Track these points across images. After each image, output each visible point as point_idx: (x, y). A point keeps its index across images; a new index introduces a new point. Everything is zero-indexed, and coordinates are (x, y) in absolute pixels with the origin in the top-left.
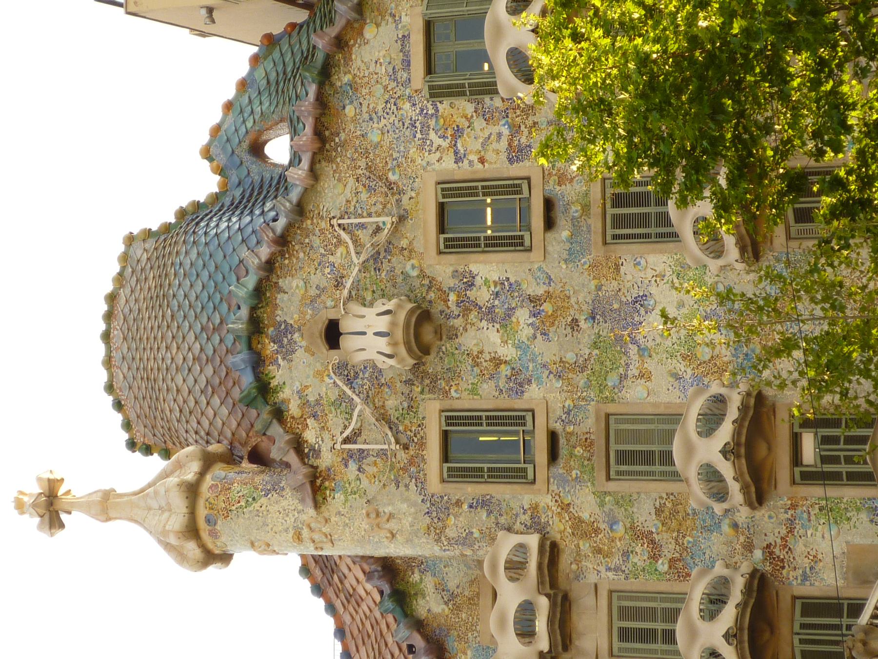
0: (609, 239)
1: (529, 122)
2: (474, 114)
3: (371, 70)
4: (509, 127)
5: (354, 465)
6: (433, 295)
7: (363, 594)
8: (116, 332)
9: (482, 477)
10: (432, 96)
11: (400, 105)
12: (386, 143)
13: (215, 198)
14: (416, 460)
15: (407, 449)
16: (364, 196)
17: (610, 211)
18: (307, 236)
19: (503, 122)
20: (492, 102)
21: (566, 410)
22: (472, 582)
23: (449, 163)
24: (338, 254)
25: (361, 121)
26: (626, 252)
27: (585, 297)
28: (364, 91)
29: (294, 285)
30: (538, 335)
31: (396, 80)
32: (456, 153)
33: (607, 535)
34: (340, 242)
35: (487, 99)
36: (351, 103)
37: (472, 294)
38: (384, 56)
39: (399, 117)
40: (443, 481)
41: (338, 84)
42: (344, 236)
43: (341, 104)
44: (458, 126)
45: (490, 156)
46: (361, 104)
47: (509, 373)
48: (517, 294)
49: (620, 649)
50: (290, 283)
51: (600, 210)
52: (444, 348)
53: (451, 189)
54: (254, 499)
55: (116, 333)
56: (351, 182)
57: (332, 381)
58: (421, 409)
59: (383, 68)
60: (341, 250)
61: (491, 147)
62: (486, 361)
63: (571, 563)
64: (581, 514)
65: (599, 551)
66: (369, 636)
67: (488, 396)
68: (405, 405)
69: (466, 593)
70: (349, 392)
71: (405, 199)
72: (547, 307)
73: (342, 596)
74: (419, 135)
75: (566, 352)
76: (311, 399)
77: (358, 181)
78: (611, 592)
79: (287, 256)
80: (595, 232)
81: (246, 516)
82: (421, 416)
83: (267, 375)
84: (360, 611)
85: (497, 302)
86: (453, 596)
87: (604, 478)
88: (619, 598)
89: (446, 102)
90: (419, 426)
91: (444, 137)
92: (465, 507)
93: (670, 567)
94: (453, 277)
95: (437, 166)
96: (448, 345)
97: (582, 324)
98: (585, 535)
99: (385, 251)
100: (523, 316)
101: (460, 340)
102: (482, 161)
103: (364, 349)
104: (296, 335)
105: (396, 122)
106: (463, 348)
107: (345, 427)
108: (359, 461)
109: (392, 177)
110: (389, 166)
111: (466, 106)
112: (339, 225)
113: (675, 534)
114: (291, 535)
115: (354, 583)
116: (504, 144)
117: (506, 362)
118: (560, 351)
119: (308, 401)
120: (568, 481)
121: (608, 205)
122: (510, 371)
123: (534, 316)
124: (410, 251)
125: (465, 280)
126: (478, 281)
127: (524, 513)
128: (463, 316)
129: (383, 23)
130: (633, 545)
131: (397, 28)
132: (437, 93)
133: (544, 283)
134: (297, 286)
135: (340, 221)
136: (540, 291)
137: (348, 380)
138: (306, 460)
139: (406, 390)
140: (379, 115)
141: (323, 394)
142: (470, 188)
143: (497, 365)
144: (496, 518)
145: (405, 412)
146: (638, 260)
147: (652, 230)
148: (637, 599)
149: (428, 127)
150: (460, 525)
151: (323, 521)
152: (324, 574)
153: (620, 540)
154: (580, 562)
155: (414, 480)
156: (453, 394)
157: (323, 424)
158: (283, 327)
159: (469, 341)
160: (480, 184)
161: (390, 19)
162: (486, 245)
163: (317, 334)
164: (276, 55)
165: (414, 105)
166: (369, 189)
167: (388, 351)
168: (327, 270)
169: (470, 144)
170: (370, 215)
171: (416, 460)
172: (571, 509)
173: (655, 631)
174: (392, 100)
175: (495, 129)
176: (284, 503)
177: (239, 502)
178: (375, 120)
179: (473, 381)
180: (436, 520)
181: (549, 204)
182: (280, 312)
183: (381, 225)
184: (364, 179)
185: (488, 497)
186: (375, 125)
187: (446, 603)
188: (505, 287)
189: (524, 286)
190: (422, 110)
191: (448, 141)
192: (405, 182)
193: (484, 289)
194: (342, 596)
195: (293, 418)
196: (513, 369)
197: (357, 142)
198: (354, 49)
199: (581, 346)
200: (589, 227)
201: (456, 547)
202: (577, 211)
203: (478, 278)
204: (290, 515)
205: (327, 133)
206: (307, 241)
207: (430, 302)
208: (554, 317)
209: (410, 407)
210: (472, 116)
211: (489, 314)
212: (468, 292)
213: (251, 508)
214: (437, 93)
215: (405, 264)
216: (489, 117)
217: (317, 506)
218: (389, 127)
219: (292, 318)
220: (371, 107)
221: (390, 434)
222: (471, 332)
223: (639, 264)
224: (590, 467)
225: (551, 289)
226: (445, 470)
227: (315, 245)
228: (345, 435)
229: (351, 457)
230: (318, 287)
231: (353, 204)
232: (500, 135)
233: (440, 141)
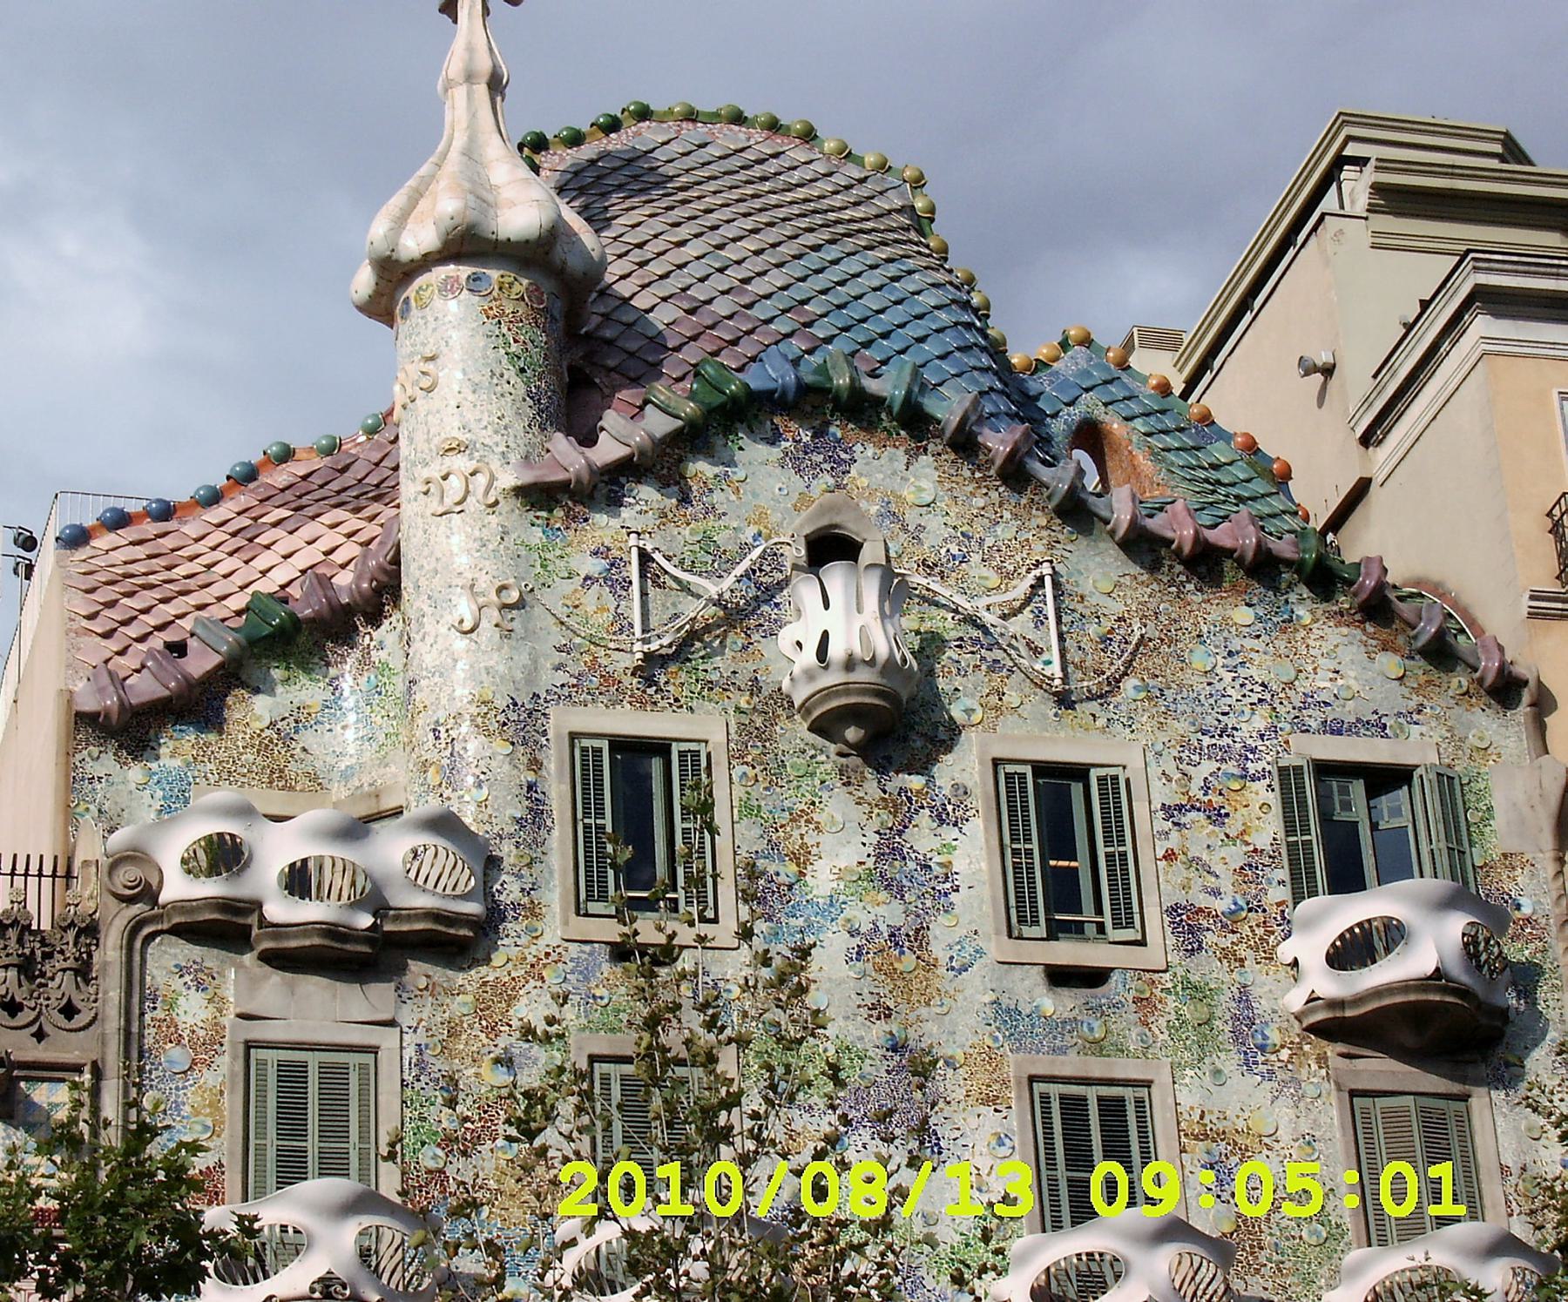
0: (1039, 1088)
1: (1242, 951)
2: (1251, 848)
3: (1321, 661)
4: (1232, 913)
5: (599, 569)
6: (919, 744)
7: (261, 562)
8: (742, 136)
9: (586, 814)
10: (1283, 771)
11: (1263, 710)
12: (1189, 678)
13: (996, 350)
14: (613, 689)
15: (633, 674)
16: (1093, 630)
17: (1092, 1093)
18: (1016, 516)
19: (1241, 903)
20: (1275, 883)
21: (721, 984)
22: (313, 778)
23: (1164, 794)
24: (985, 572)
25: (1225, 634)
26: (1016, 1119)
27: (931, 1035)
28: (1281, 644)
29: (924, 484)
30: (857, 941)
31: (1305, 706)
32: (1180, 808)
33: (485, 1050)
34: (1009, 576)
35: (1283, 874)
36: (1259, 619)
37: (924, 818)
38: (1349, 687)
39: (1238, 707)
40: (573, 736)
41: (1293, 597)
42: (1022, 587)
43: (1255, 600)
44: (1227, 815)
45: (1178, 872)
46: (1258, 637)
47: (782, 879)
48: (929, 903)
49: (262, 1063)
50: (926, 477)
51: (1097, 1073)
52: (823, 758)
53: (1116, 792)
54: (522, 370)
55: (733, 137)
56: (1117, 608)
57: (750, 540)
58: (710, 706)
59: (1328, 684)
60: (994, 580)
61: (1192, 874)
62: (802, 836)
63: (428, 976)
64: (524, 1000)
65: (453, 1033)
66: (169, 568)
67: (736, 837)
68: (714, 677)
69: (292, 766)
70: (740, 570)
71: (1094, 706)
72: (909, 961)
73: (244, 521)
74: (1206, 741)
75: (828, 991)
76: (717, 497)
77: (1119, 619)
78: (373, 1050)
79: (978, 475)
80: (1053, 1062)
81: (490, 351)
82: (694, 704)
83: (756, 416)
84: (217, 555)
85: (911, 865)
86: (287, 740)
87: (596, 1051)
88: (363, 1067)
89: (1274, 799)
90: (676, 700)
91: (1206, 788)
92: (531, 777)
93: (429, 1172)
94: (956, 786)
95: (1155, 771)
96: (828, 767)
97: (881, 1027)
98: (481, 1009)
99: (996, 661)
100: (891, 913)
101: (840, 791)
102: (1170, 856)
103: (827, 606)
104: (831, 481)
105: (1228, 701)
106: (825, 795)
107: (668, 558)
108: (605, 579)
109: (1129, 684)
110: (1151, 682)
111: (1268, 830)
112: (1041, 579)
113: (492, 1184)
114: (455, 433)
115: (281, 548)
116: (1203, 901)
117: (802, 874)
118: (830, 979)
119: (711, 491)
120: (587, 979)
121: (1106, 1091)
122: (787, 880)
123: (892, 935)
124: (997, 708)
125: (950, 808)
126: (950, 833)
127: (523, 890)
128: (883, 799)
129: (1406, 691)
130: (469, 1101)
131: (1399, 714)
132: (1288, 778)
133: (952, 958)
134: (920, 489)
135: (1048, 580)
136: (938, 950)
137: (754, 572)
138: (606, 478)
139: (742, 680)
140: (1240, 669)
141: (724, 521)
142: (1121, 831)
143: (795, 857)
144: (511, 836)
145: (701, 675)
146: (1007, 1141)
147: (1062, 1173)
148: (363, 1105)
149: (1223, 760)
150: (494, 764)
151: (491, 500)
152: (282, 490)
153: (477, 1075)
154: (432, 995)
155: (575, 681)
156: (739, 770)
157: (670, 515)
158: (843, 456)
159: (837, 806)
160: (1129, 848)
161: (1412, 705)
162: (1016, 853)
163: (837, 520)
164: (1259, 487)
165: (1262, 736)
166: (1106, 639)
167: (836, 651)
168: (954, 550)
169: (1199, 834)
170: (1061, 637)
171: (613, 689)
172: (532, 983)
173: (303, 1136)
174: (1268, 697)
175: (1226, 883)
176: (519, 427)
177: (516, 341)
178: (1229, 661)
179: (764, 809)
180: (501, 718)
181: (1094, 977)
182: (870, 453)
183: (1045, 657)
184: (1122, 632)
185: (549, 823)
186: (1221, 661)
187: (272, 724)
188: (941, 886)
189: (943, 919)
190: (1253, 751)
191: (1200, 795)
192: (1123, 708)
193: (936, 843)
194: (244, 521)
195: (681, 460)
196: (790, 887)
197: (1187, 625)
198: (1358, 632)
199: (841, 1022)
200: (1062, 1051)
201: (448, 753)
202: (1091, 1030)
203: (955, 833)
204: (498, 438)
205: (1203, 569)
206: (1007, 515)
207: (905, 739)
208: (892, 973)
209: (710, 685)
210: (1248, 844)
211: (890, 848)
212: (927, 811)
213: (505, 361)
214: (1288, 778)
215: (973, 696)
216: (1249, 871)
217: (521, 492)
218: (1219, 686)
219: (861, 475)
220: (1253, 655)
221: (665, 641)
222: (858, 814)
223: (1001, 1144)
224: (616, 1024)
225: (942, 971)
226: (596, 743)
227: (999, 529)
228: (657, 556)
229: (612, 565)
230: (921, 528)
231: (1080, 608)
232: (1216, 893)
233: (1197, 783)
